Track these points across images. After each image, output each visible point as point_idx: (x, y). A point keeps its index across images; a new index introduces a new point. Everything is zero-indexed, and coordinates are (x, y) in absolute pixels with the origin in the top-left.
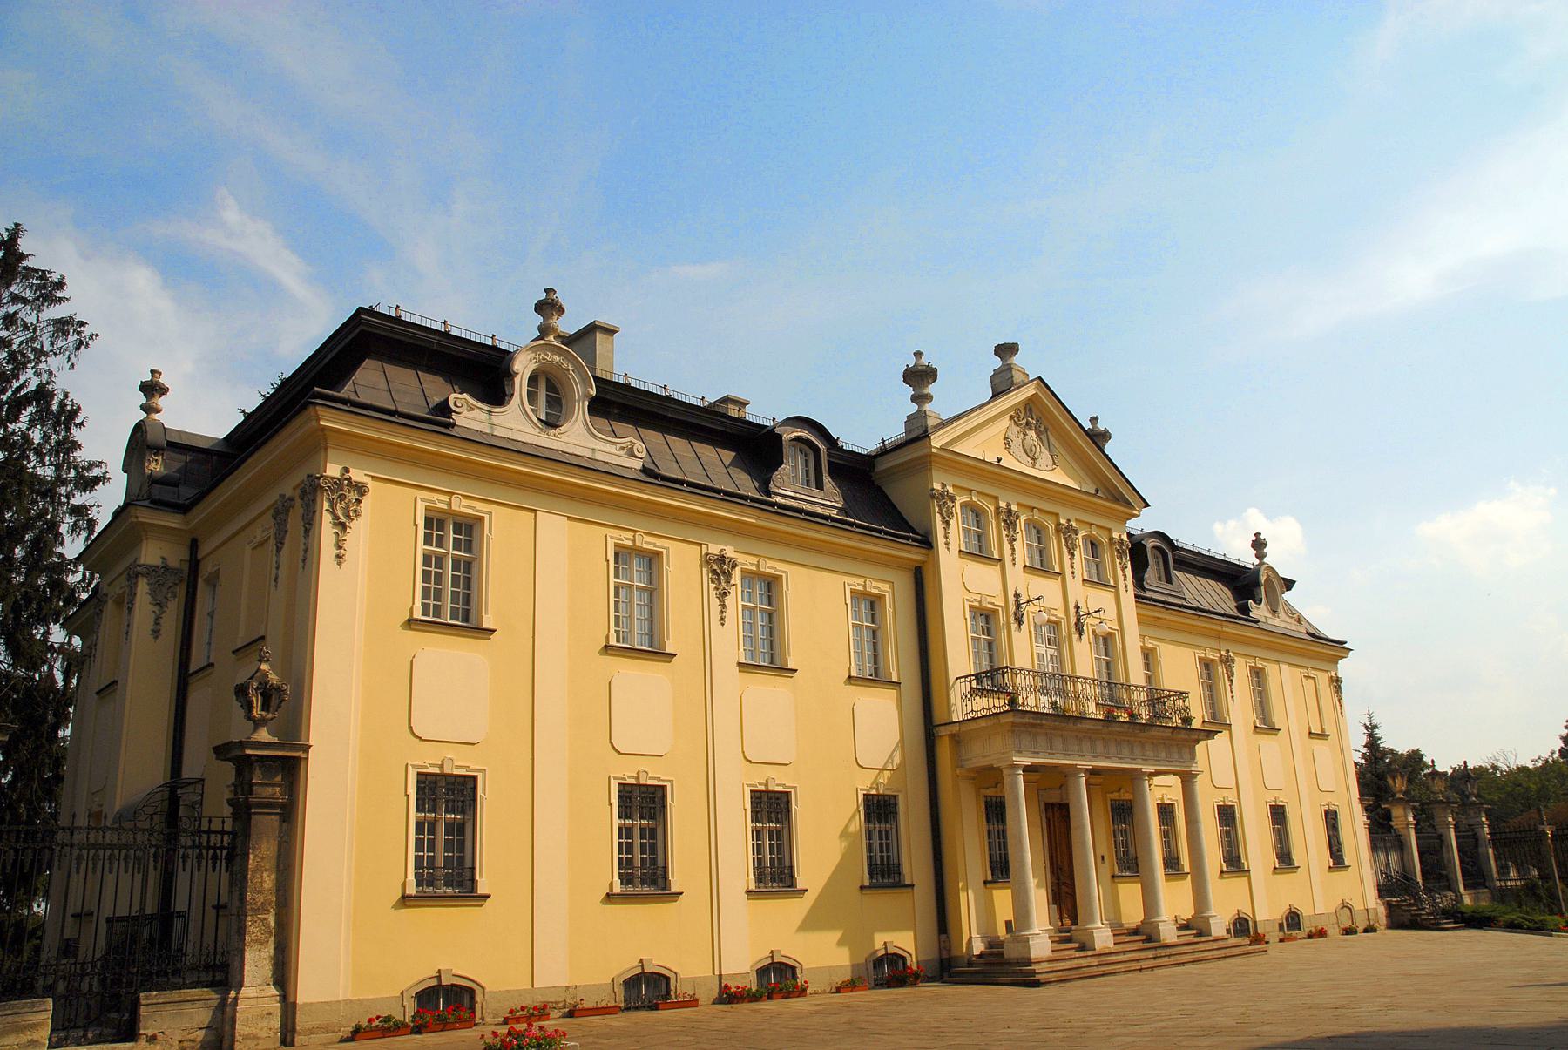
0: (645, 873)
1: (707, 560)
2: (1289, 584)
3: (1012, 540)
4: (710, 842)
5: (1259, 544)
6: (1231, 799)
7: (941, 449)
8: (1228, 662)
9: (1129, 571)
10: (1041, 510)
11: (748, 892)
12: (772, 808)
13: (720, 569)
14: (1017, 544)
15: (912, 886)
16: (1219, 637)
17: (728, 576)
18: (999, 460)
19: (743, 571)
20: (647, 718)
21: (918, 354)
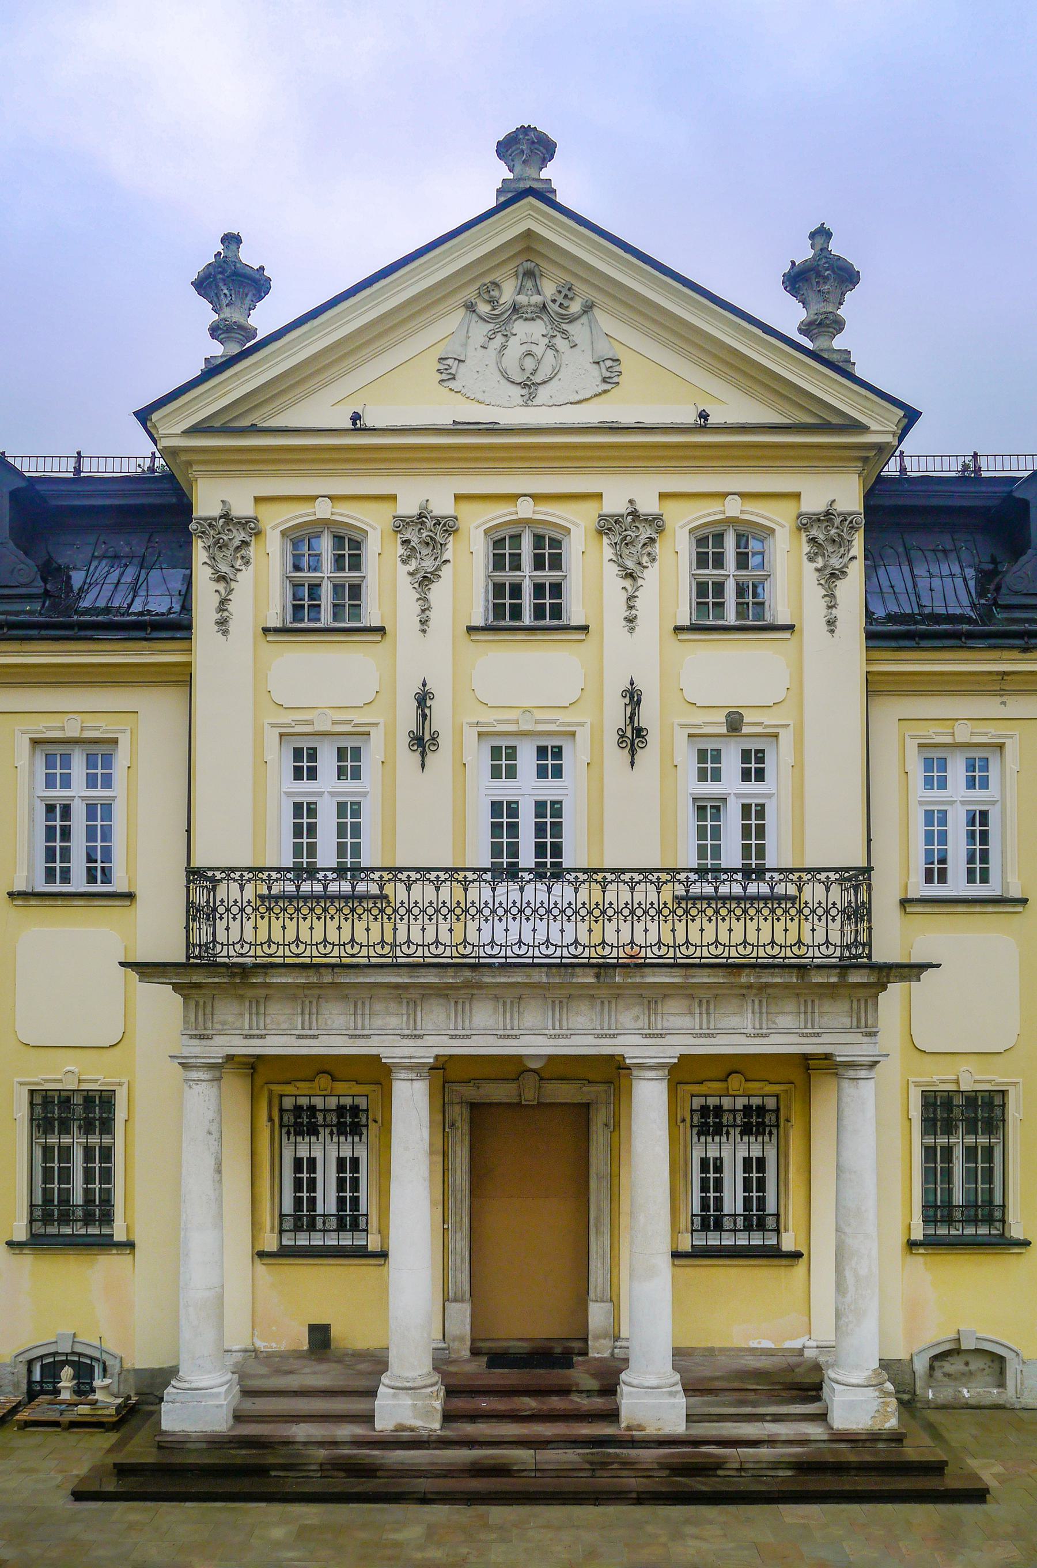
3: (425, 581)
9: (852, 588)
10: (535, 497)
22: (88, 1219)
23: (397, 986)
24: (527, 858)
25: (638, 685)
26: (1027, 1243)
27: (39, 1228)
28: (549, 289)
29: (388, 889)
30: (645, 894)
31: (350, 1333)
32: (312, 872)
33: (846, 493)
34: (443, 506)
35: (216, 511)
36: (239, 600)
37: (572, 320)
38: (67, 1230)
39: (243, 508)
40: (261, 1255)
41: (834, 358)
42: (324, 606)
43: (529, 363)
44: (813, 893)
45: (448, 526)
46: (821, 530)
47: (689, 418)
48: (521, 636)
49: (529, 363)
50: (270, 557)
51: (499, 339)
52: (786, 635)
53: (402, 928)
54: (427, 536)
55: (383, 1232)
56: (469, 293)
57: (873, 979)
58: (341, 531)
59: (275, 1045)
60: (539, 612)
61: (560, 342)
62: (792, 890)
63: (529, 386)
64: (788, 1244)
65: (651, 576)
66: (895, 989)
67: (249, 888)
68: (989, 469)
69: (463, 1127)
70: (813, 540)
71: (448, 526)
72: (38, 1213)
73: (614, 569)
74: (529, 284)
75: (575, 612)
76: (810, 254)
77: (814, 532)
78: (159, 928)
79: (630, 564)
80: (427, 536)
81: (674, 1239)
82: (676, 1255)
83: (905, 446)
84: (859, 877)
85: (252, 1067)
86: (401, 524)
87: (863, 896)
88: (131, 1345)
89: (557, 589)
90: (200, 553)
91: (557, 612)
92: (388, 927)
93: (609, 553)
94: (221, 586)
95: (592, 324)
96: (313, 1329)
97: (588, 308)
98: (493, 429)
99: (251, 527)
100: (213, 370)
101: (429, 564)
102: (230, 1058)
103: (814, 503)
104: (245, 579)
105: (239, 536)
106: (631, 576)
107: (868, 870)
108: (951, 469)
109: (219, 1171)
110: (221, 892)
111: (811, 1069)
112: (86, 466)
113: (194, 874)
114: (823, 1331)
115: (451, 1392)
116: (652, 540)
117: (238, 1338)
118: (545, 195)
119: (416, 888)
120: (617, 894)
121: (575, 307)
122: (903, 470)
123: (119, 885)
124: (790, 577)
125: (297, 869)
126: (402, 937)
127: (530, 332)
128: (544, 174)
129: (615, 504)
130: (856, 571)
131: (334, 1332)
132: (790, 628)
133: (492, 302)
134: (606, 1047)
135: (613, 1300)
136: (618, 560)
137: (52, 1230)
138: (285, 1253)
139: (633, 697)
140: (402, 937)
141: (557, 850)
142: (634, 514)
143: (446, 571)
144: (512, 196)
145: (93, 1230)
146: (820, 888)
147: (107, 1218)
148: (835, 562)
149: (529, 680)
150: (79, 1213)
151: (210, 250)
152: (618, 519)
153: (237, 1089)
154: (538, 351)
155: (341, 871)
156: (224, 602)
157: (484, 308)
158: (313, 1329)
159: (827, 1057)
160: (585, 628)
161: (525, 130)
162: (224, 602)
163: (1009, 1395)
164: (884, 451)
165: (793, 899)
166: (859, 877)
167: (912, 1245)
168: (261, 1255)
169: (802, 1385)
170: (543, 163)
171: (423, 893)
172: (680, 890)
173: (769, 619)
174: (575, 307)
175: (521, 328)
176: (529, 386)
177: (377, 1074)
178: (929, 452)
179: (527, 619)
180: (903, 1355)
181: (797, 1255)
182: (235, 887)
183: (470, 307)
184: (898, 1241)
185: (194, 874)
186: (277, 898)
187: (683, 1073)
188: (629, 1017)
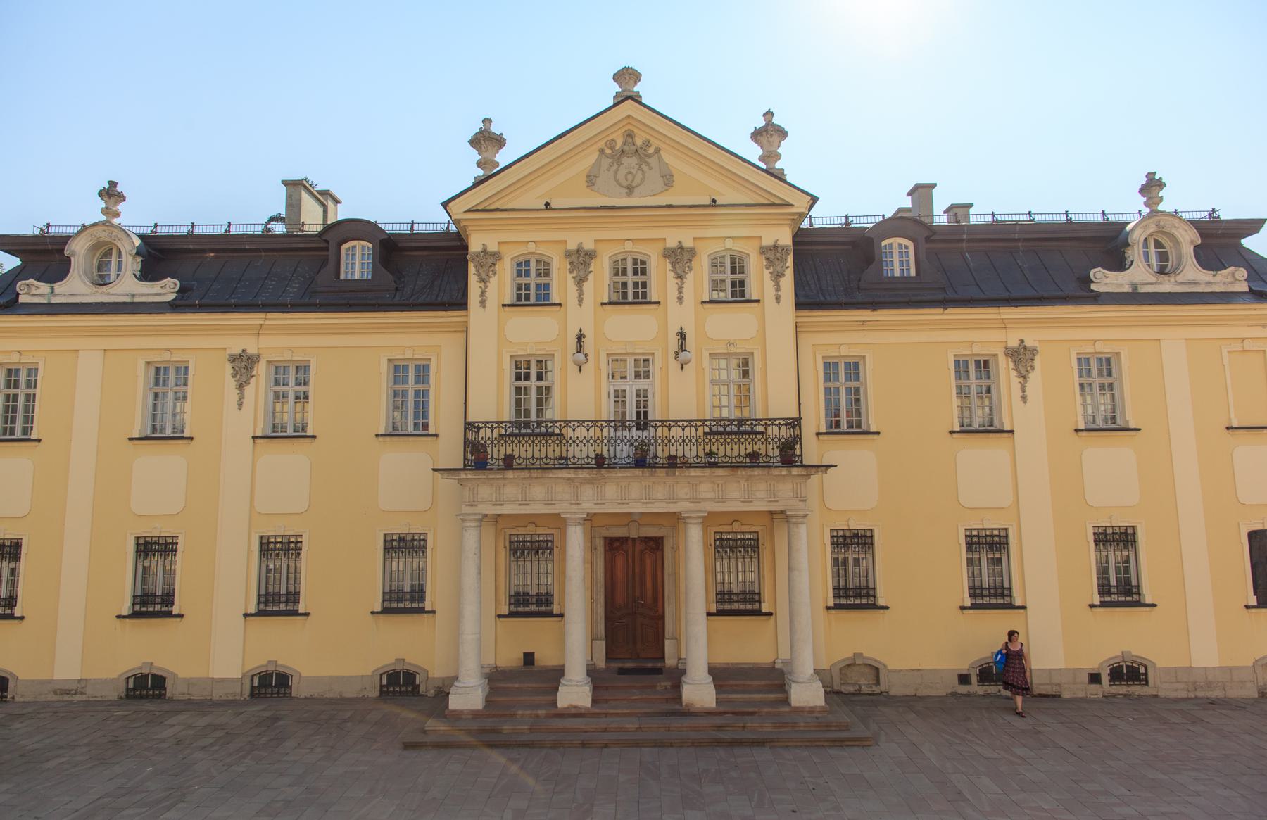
0: (153, 604)
1: (233, 359)
2: (1253, 226)
3: (580, 281)
4: (218, 580)
5: (1152, 187)
6: (993, 523)
7: (469, 211)
8: (1022, 356)
9: (788, 282)
11: (246, 615)
12: (281, 549)
13: (244, 365)
14: (588, 286)
15: (433, 612)
16: (1004, 325)
17: (249, 369)
18: (547, 204)
19: (269, 362)
20: (158, 489)
21: (487, 121)
22: (412, 600)
23: (569, 479)
24: (631, 413)
25: (685, 330)
26: (887, 608)
27: (387, 604)
28: (639, 142)
29: (564, 431)
30: (690, 432)
31: (545, 658)
32: (527, 425)
33: (786, 239)
34: (589, 246)
35: (479, 249)
36: (489, 292)
37: (650, 156)
38: (401, 605)
39: (492, 248)
40: (500, 616)
41: (776, 173)
42: (531, 294)
43: (630, 177)
44: (773, 431)
45: (591, 255)
46: (771, 254)
47: (708, 201)
48: (627, 307)
49: (630, 177)
50: (506, 269)
51: (615, 166)
52: (756, 304)
53: (571, 449)
54: (581, 260)
55: (562, 604)
56: (601, 144)
57: (804, 473)
58: (539, 258)
59: (507, 509)
60: (636, 295)
61: (644, 166)
62: (762, 429)
63: (630, 190)
64: (765, 609)
65: (690, 277)
66: (815, 478)
67: (496, 431)
68: (857, 223)
69: (601, 549)
70: (768, 259)
71: (591, 255)
72: (387, 597)
73: (672, 274)
74: (629, 140)
75: (653, 295)
76: (763, 123)
77: (769, 255)
78: (450, 449)
79: (680, 272)
80: (581, 260)
81: (707, 607)
82: (709, 614)
83: (813, 213)
84: (795, 423)
85: (497, 518)
86: (568, 254)
87: (797, 432)
88: (432, 666)
89: (644, 285)
90: (472, 269)
91: (644, 295)
92: (564, 449)
93: (669, 266)
94: (482, 285)
95: (660, 158)
96: (525, 654)
97: (657, 151)
98: (613, 208)
99: (497, 256)
100: (479, 182)
101: (582, 273)
102: (486, 515)
103: (768, 242)
104: (494, 281)
105: (490, 261)
106: (680, 277)
107: (799, 419)
108: (837, 223)
109: (480, 573)
110: (482, 431)
111: (778, 518)
112: (416, 227)
113: (469, 425)
114: (784, 654)
115: (595, 689)
116: (690, 260)
117: (490, 660)
118: (636, 99)
119: (578, 430)
120: (676, 432)
121: (651, 150)
122: (811, 224)
123: (432, 431)
124: (758, 278)
125: (515, 422)
126: (570, 455)
127: (630, 162)
128: (636, 89)
129: (672, 244)
130: (789, 273)
131: (536, 656)
132: (758, 301)
133: (612, 149)
134: (672, 508)
135: (676, 639)
136: (674, 270)
137: (394, 605)
138: (512, 615)
139: (682, 336)
140: (570, 455)
141: (646, 413)
142: (681, 248)
143: (591, 277)
144: (620, 100)
145: (415, 605)
146: (776, 428)
147: (422, 599)
148: (779, 269)
149: (633, 329)
150: (408, 596)
151: (476, 127)
152: (673, 251)
153: (489, 531)
154: (634, 171)
155: (539, 424)
156: (483, 293)
157: (608, 151)
158: (525, 654)
159: (782, 512)
160: (658, 303)
161: (627, 68)
162: (483, 293)
163: (882, 687)
164: (802, 216)
165: (763, 433)
166: (795, 423)
167: (828, 608)
168: (500, 616)
169: (775, 679)
170: (636, 83)
171: (581, 432)
172: (707, 430)
173: (747, 297)
174: (651, 150)
175: (626, 161)
176: (630, 190)
177: (559, 522)
178: (825, 215)
179: (630, 298)
180: (826, 667)
181: (770, 614)
182: (489, 431)
183: (602, 151)
184: (821, 606)
185: (469, 425)
186: (509, 435)
187: (709, 520)
188: (683, 491)
